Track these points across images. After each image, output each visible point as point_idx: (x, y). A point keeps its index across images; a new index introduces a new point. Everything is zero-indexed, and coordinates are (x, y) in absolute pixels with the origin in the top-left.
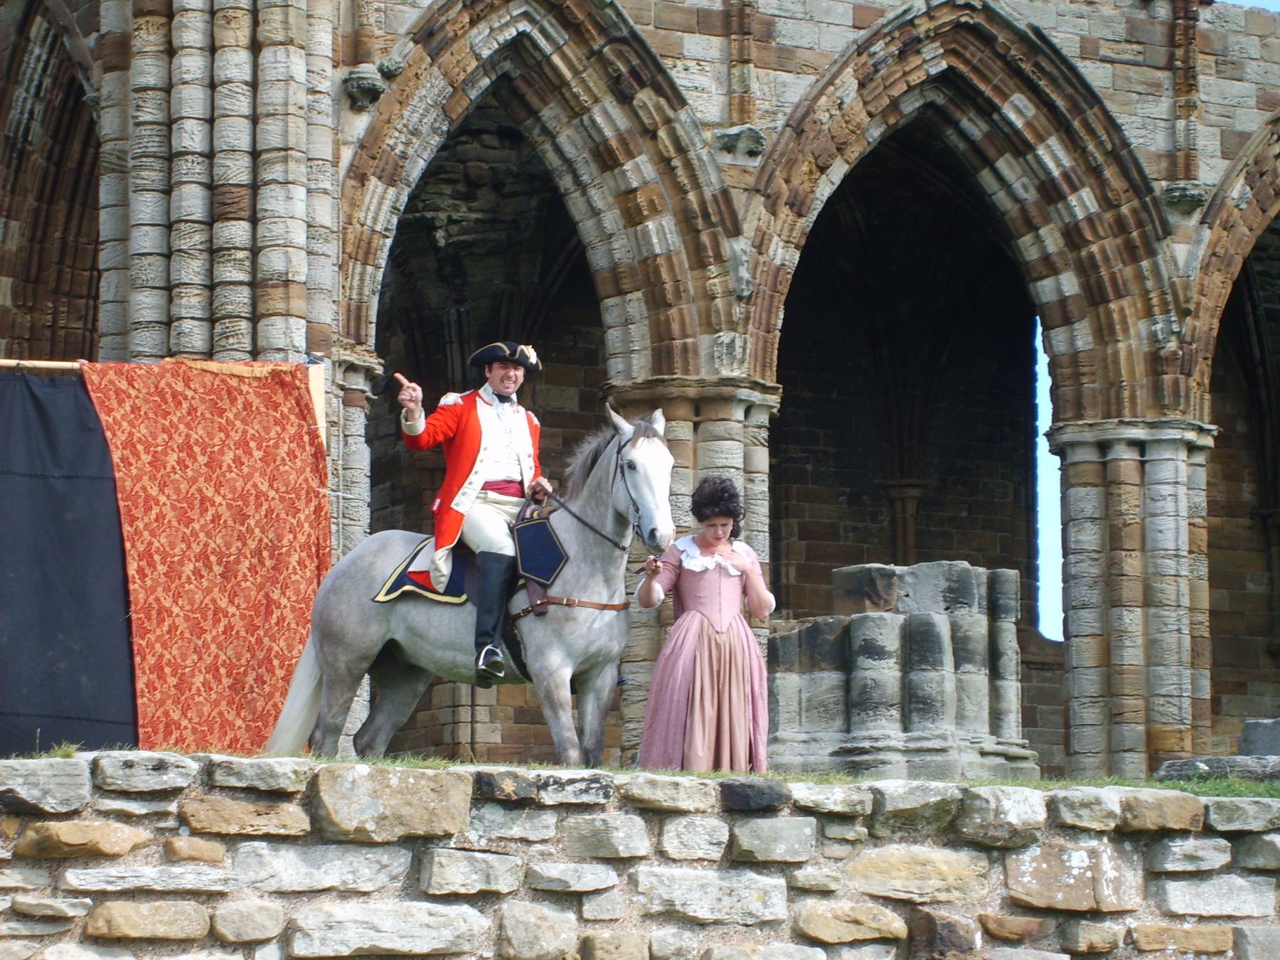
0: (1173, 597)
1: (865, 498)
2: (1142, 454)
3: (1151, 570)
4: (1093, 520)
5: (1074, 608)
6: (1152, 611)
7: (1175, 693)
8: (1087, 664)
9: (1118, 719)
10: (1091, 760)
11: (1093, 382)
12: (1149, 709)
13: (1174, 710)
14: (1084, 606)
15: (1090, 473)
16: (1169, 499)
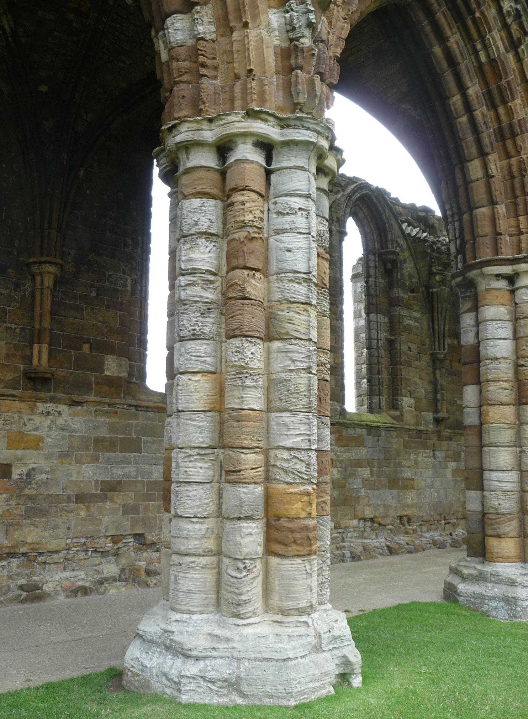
0: (302, 329)
1: (10, 270)
2: (269, 160)
3: (277, 296)
4: (208, 235)
5: (182, 339)
6: (276, 345)
7: (304, 445)
8: (194, 407)
9: (233, 477)
10: (197, 526)
11: (215, 78)
12: (267, 465)
13: (302, 467)
14: (195, 337)
15: (208, 182)
16: (299, 213)
